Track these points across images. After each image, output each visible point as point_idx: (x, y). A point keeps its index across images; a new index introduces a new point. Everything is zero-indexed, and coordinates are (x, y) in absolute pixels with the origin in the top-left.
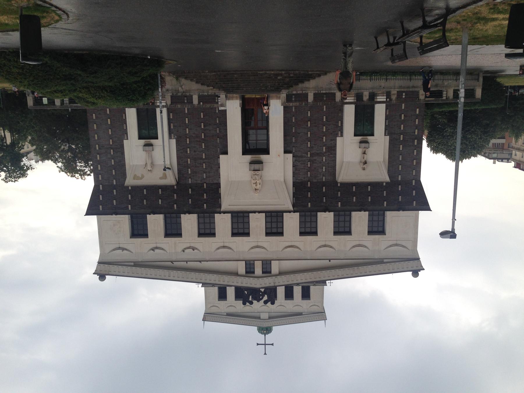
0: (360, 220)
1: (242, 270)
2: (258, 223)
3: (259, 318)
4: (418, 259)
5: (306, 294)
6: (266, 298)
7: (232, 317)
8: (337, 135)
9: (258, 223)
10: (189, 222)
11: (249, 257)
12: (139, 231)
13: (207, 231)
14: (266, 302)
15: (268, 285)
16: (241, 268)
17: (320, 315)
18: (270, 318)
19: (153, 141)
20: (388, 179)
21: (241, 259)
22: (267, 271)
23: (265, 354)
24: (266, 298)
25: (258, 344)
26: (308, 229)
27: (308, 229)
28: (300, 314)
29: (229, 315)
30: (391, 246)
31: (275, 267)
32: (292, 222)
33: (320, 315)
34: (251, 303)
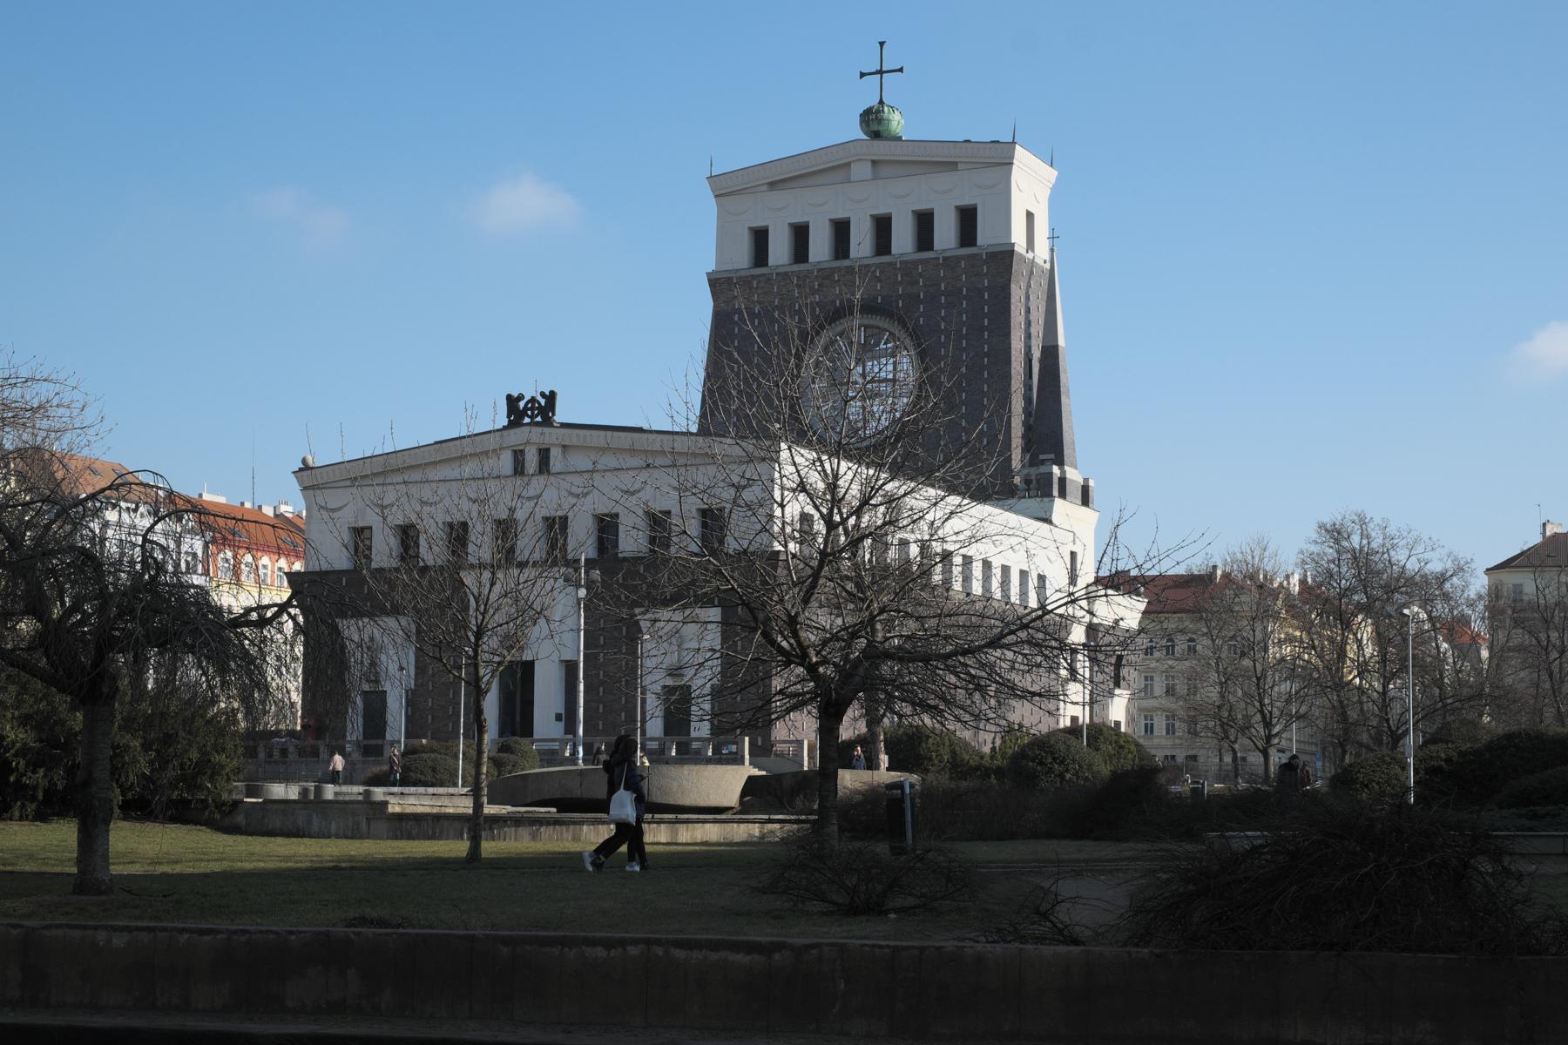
0: (384, 551)
1: (555, 453)
2: (529, 544)
3: (874, 162)
4: (305, 489)
5: (760, 238)
6: (522, 404)
7: (941, 160)
8: (414, 692)
9: (529, 544)
10: (632, 541)
11: (542, 479)
12: (713, 521)
13: (607, 527)
14: (521, 397)
15: (518, 430)
16: (556, 462)
17: (727, 188)
18: (849, 164)
19: (669, 682)
20: (342, 624)
21: (552, 479)
22: (519, 456)
23: (882, 44)
24: (522, 404)
25: (901, 70)
26: (458, 535)
27: (458, 535)
28: (773, 185)
29: (952, 166)
30: (340, 509)
31: (506, 462)
32: (481, 546)
33: (727, 188)
34: (543, 394)
